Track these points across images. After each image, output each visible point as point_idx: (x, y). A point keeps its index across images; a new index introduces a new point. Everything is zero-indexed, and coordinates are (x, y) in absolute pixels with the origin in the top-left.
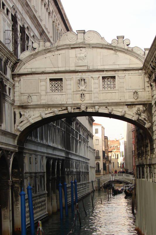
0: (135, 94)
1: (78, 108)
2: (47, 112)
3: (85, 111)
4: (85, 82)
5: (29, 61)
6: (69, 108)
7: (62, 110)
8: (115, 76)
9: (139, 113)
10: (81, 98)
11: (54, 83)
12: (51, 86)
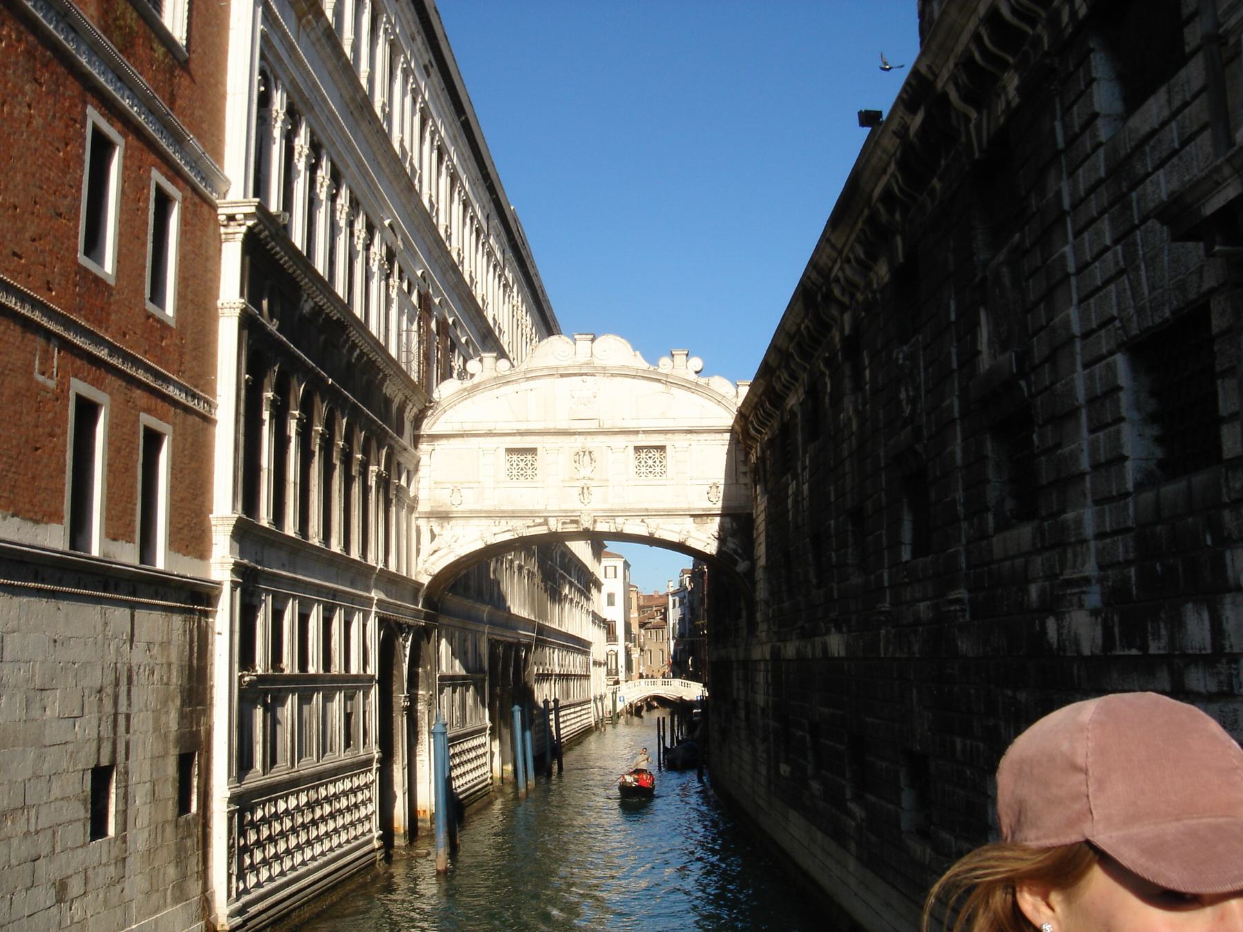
0: (714, 490)
1: (572, 522)
2: (496, 530)
3: (591, 529)
4: (592, 460)
5: (455, 405)
7: (535, 526)
12: (508, 465)
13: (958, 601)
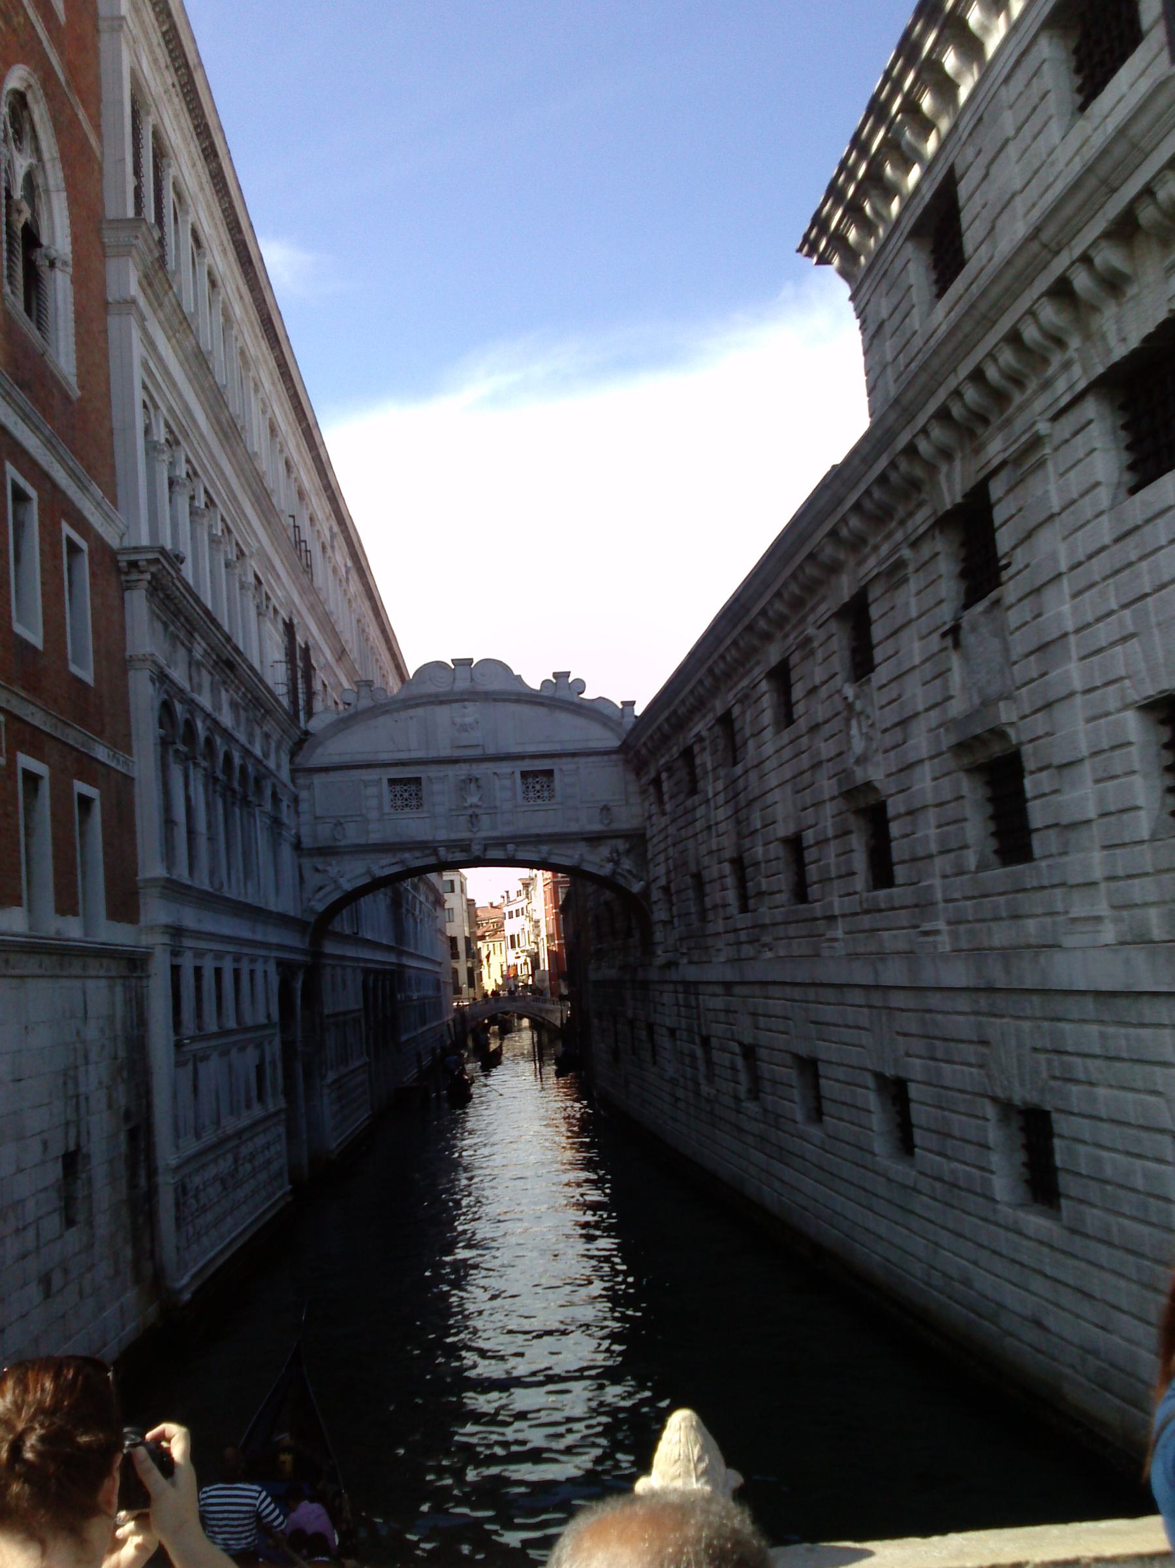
1: (462, 851)
2: (384, 862)
4: (478, 787)
6: (442, 851)
9: (616, 858)
13: (936, 932)
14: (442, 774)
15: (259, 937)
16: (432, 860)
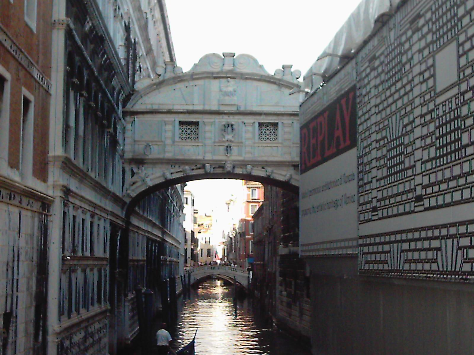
1: (220, 167)
2: (172, 171)
4: (233, 129)
7: (197, 169)
8: (278, 123)
10: (226, 153)
11: (185, 127)
14: (212, 120)
15: (103, 205)
16: (201, 172)
